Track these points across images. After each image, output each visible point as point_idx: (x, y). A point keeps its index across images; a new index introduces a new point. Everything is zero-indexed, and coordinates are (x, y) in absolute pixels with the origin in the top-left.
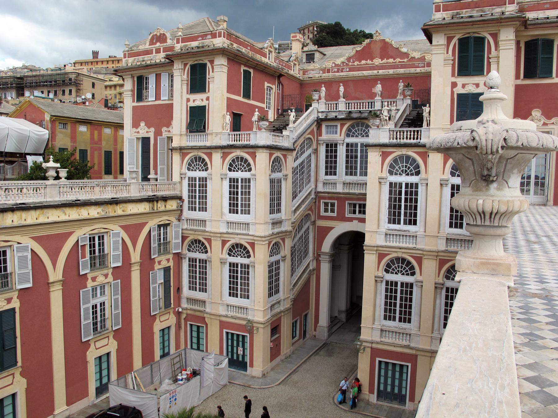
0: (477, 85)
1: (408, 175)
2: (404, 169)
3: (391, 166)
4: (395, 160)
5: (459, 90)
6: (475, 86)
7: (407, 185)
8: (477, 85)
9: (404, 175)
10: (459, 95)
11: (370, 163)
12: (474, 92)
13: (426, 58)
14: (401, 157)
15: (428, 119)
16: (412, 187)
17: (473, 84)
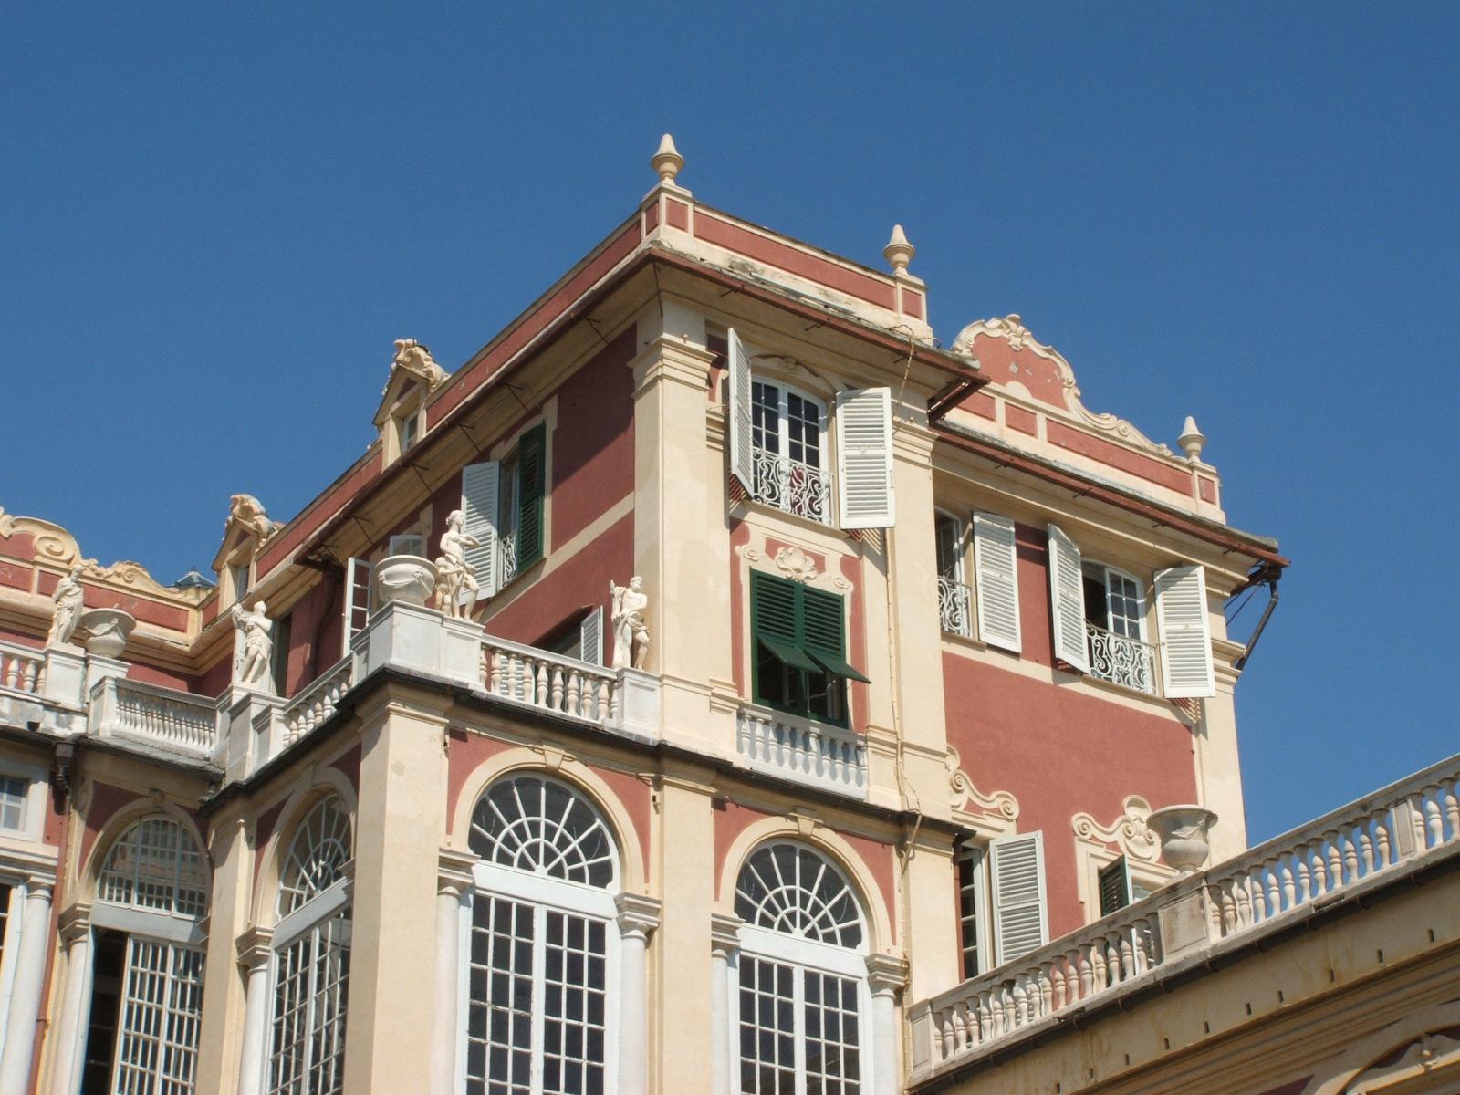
0: (820, 563)
1: (557, 872)
2: (542, 840)
3: (481, 812)
4: (498, 790)
5: (756, 557)
6: (811, 562)
7: (554, 920)
8: (820, 563)
9: (541, 870)
10: (760, 580)
11: (400, 769)
12: (810, 584)
13: (42, 547)
14: (527, 779)
15: (642, 636)
16: (576, 940)
17: (806, 553)
